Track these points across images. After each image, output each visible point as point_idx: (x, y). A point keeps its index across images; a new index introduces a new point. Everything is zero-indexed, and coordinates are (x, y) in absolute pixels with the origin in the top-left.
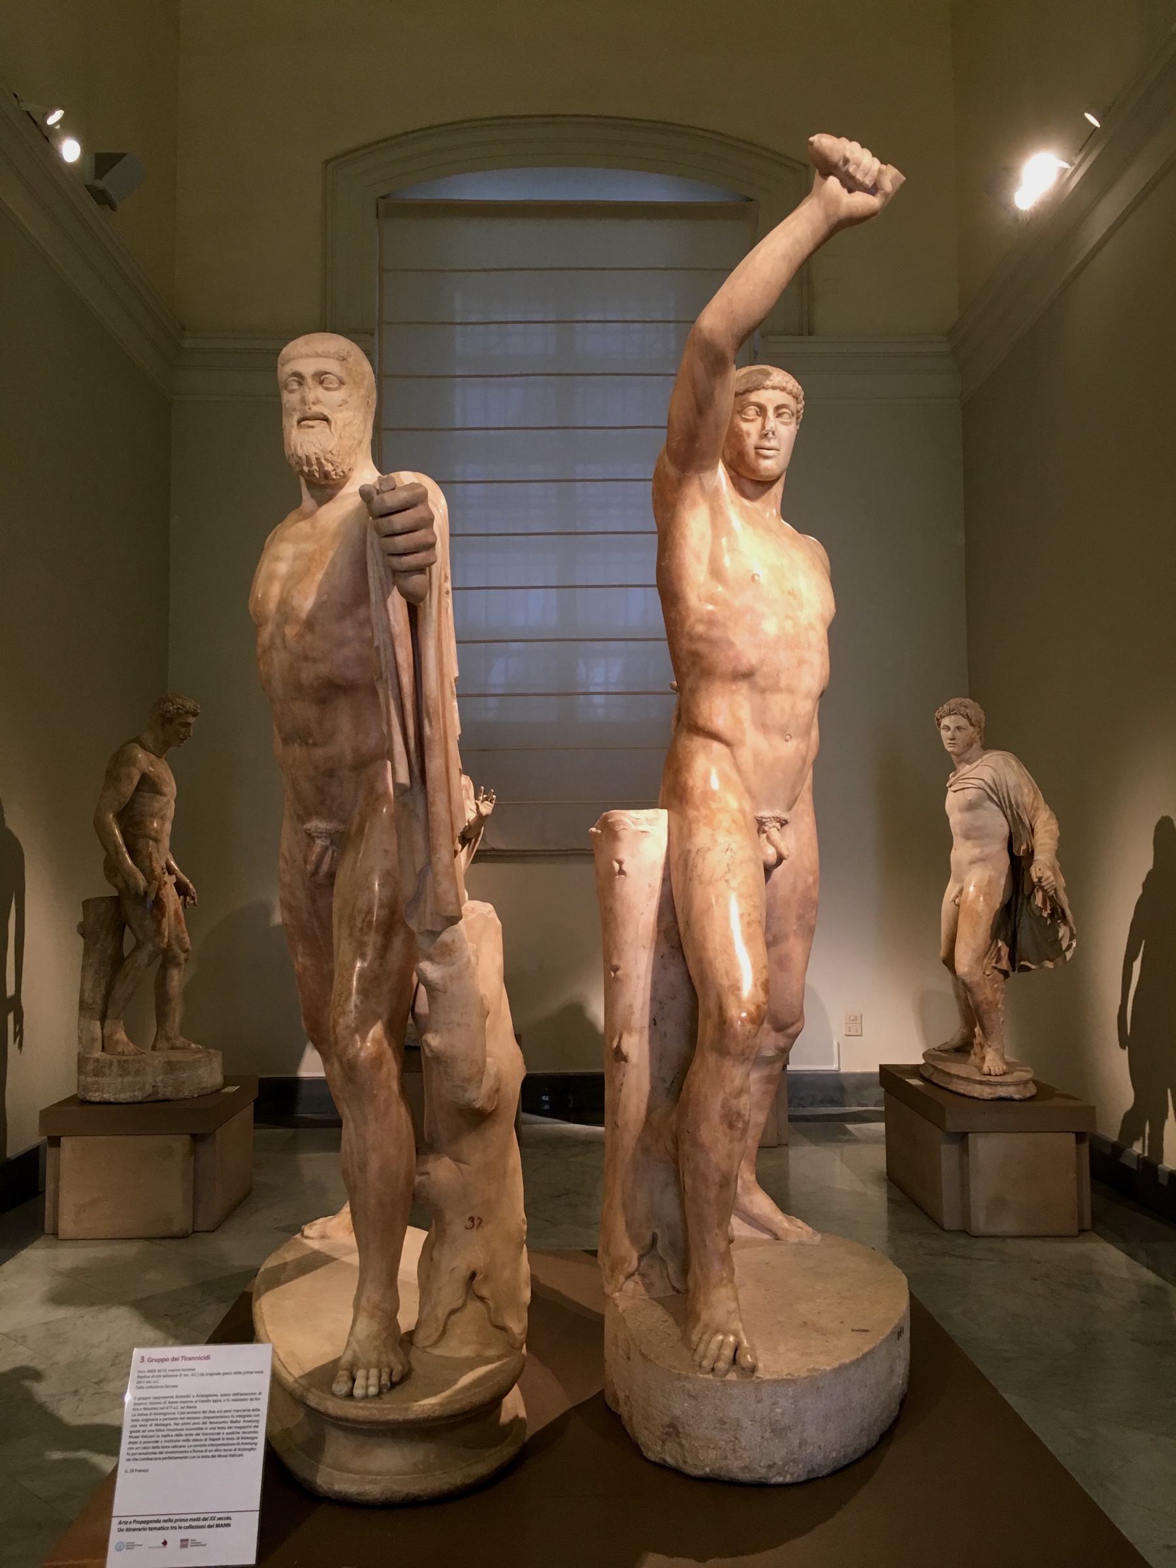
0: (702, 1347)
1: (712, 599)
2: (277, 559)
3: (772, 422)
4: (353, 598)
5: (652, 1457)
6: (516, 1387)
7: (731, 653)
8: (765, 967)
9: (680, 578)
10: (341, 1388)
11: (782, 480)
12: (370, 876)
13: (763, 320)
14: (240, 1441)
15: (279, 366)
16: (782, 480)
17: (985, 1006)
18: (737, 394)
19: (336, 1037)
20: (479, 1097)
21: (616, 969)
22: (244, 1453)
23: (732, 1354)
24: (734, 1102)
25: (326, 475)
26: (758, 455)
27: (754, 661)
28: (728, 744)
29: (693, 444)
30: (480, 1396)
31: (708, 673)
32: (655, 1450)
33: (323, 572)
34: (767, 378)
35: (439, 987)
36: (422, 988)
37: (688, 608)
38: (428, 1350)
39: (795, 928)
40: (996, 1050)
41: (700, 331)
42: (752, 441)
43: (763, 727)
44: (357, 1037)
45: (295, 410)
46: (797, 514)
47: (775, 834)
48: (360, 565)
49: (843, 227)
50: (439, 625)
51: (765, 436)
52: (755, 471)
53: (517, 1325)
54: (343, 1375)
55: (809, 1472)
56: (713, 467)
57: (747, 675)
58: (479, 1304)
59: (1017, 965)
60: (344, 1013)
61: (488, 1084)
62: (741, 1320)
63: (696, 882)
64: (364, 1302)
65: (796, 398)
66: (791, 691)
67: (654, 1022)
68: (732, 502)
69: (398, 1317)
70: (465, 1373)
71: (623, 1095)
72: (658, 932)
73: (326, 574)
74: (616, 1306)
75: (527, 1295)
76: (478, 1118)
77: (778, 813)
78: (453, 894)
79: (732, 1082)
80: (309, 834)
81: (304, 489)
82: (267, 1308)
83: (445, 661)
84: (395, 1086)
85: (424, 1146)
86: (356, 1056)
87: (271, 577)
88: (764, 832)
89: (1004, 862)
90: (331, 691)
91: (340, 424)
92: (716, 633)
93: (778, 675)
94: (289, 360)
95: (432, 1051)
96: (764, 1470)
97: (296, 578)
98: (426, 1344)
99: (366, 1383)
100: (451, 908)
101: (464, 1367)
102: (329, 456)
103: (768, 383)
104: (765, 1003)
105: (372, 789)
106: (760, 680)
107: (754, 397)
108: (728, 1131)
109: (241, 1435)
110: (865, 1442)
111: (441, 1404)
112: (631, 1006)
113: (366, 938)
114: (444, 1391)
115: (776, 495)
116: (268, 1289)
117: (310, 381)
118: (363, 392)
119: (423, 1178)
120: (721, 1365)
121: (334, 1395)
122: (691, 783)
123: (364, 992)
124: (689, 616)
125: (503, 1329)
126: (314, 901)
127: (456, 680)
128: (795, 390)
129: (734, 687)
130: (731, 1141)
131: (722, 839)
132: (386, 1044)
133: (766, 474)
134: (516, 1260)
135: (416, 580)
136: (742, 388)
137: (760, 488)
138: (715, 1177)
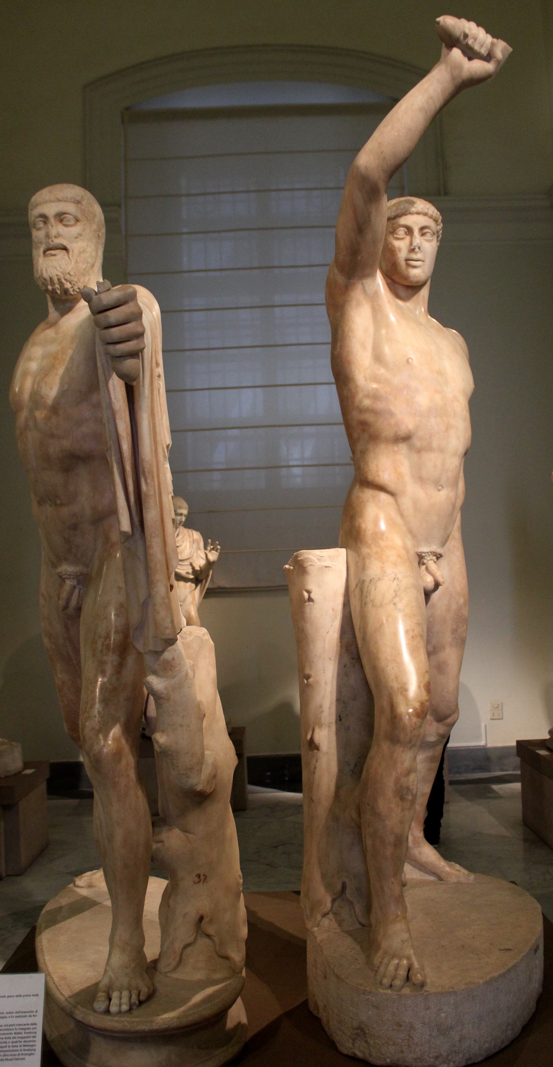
0: (382, 969)
1: (375, 379)
2: (30, 359)
3: (418, 240)
4: (88, 387)
5: (345, 1051)
6: (239, 1000)
7: (393, 421)
8: (427, 672)
9: (349, 363)
10: (100, 1005)
11: (428, 284)
12: (107, 608)
13: (405, 160)
14: (23, 1048)
15: (30, 211)
16: (428, 284)
18: (389, 219)
19: (84, 737)
20: (200, 781)
21: (308, 677)
22: (27, 1057)
23: (406, 973)
24: (403, 780)
25: (66, 291)
26: (408, 265)
27: (411, 427)
28: (392, 494)
29: (358, 257)
30: (207, 1011)
31: (375, 438)
32: (347, 1045)
33: (64, 367)
34: (413, 206)
35: (163, 696)
36: (151, 698)
37: (356, 387)
38: (169, 975)
39: (450, 640)
41: (358, 168)
42: (402, 255)
43: (420, 480)
44: (101, 736)
45: (41, 243)
46: (441, 311)
47: (432, 565)
48: (91, 359)
49: (465, 86)
50: (152, 401)
51: (412, 250)
52: (406, 278)
53: (238, 955)
54: (101, 995)
55: (467, 1060)
56: (373, 275)
57: (406, 438)
58: (207, 940)
60: (89, 718)
61: (206, 771)
62: (413, 947)
63: (370, 605)
64: (117, 938)
65: (436, 221)
66: (442, 450)
67: (339, 718)
68: (389, 302)
69: (145, 949)
70: (197, 992)
71: (316, 776)
72: (341, 647)
73: (67, 369)
74: (316, 938)
75: (244, 931)
76: (200, 798)
77: (435, 548)
78: (168, 620)
79: (402, 764)
80: (61, 577)
81: (50, 304)
82: (46, 942)
83: (158, 430)
84: (132, 774)
85: (158, 819)
86: (100, 752)
87: (25, 374)
88: (424, 564)
90: (73, 461)
91: (76, 252)
92: (380, 406)
93: (430, 437)
94: (36, 206)
95: (160, 747)
96: (432, 1060)
97: (45, 372)
98: (167, 970)
99: (120, 1002)
100: (168, 631)
101: (197, 988)
102: (68, 277)
103: (413, 210)
104: (427, 701)
105: (107, 539)
106: (417, 443)
107: (403, 221)
109: (23, 1044)
110: (510, 1035)
111: (178, 1018)
112: (321, 707)
113: (105, 658)
114: (179, 1007)
116: (47, 927)
117: (52, 220)
118: (94, 227)
119: (160, 845)
120: (398, 982)
121: (95, 1011)
122: (363, 526)
123: (105, 701)
125: (227, 958)
126: (66, 627)
127: (168, 447)
128: (434, 215)
129: (396, 449)
130: (403, 810)
131: (390, 570)
132: (123, 741)
133: (415, 280)
134: (235, 907)
135: (130, 363)
136: (393, 214)
137: (410, 291)
138: (391, 839)
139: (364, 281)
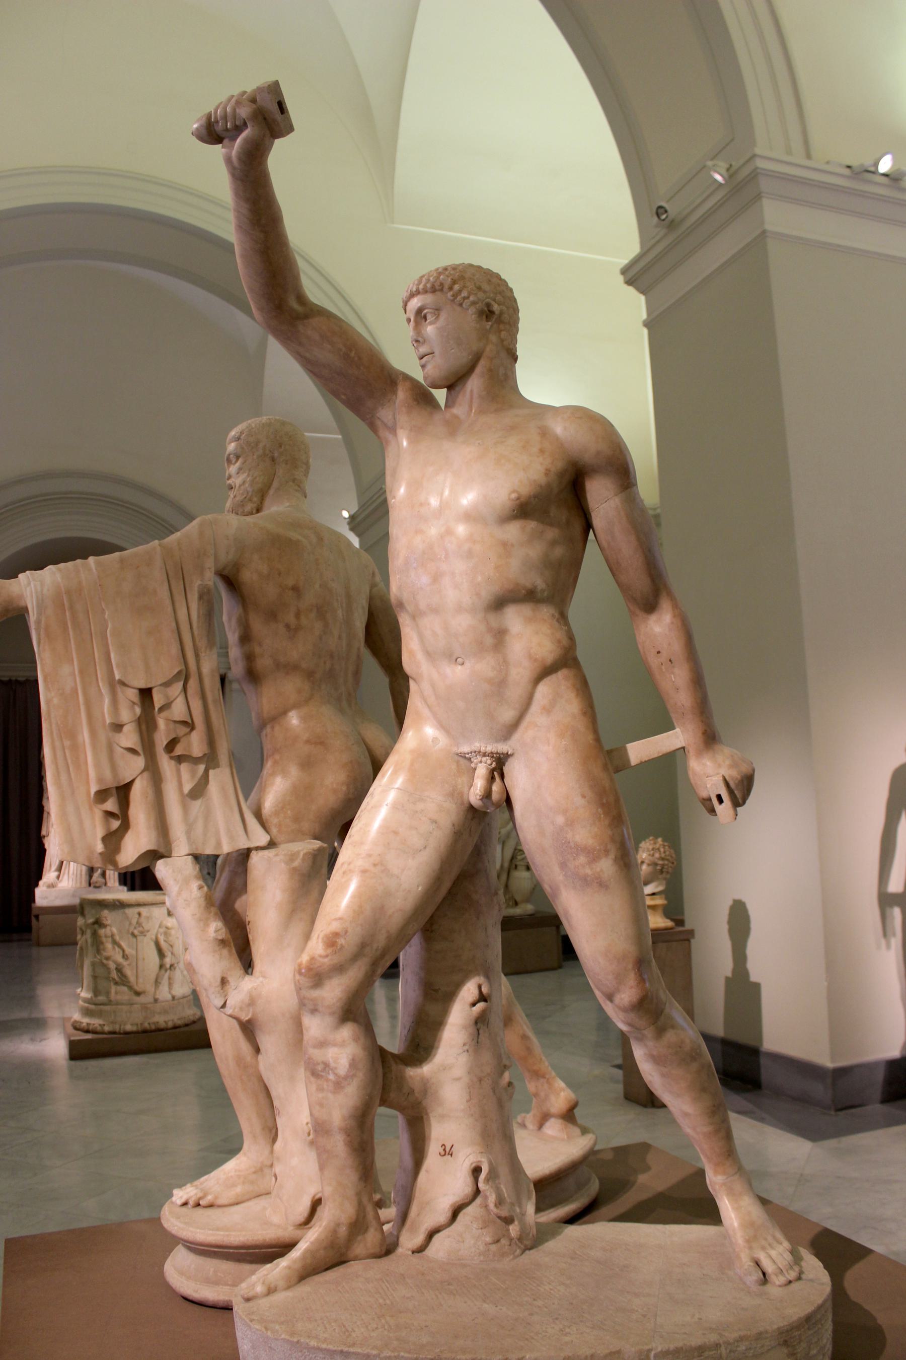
39: (561, 878)
43: (429, 654)
108: (312, 1079)
115: (472, 391)
139: (378, 415)
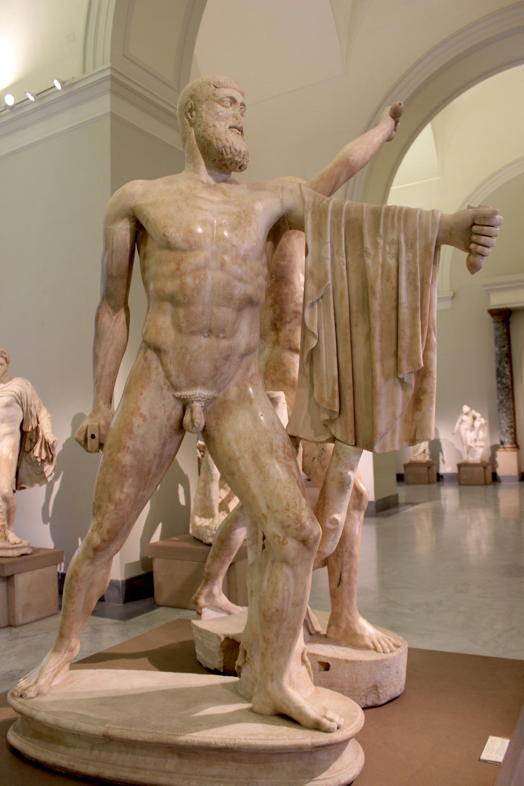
17: (13, 509)
37: (295, 289)
40: (13, 531)
59: (19, 487)
89: (18, 435)
124: (296, 293)
